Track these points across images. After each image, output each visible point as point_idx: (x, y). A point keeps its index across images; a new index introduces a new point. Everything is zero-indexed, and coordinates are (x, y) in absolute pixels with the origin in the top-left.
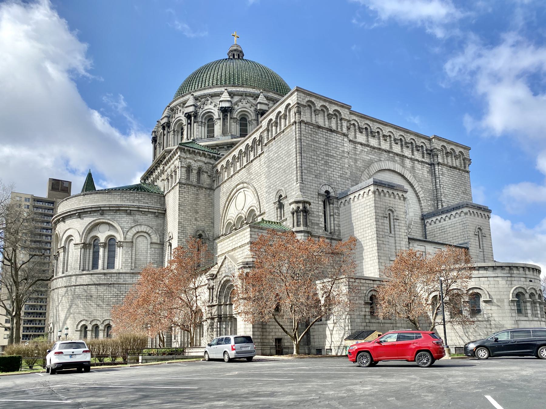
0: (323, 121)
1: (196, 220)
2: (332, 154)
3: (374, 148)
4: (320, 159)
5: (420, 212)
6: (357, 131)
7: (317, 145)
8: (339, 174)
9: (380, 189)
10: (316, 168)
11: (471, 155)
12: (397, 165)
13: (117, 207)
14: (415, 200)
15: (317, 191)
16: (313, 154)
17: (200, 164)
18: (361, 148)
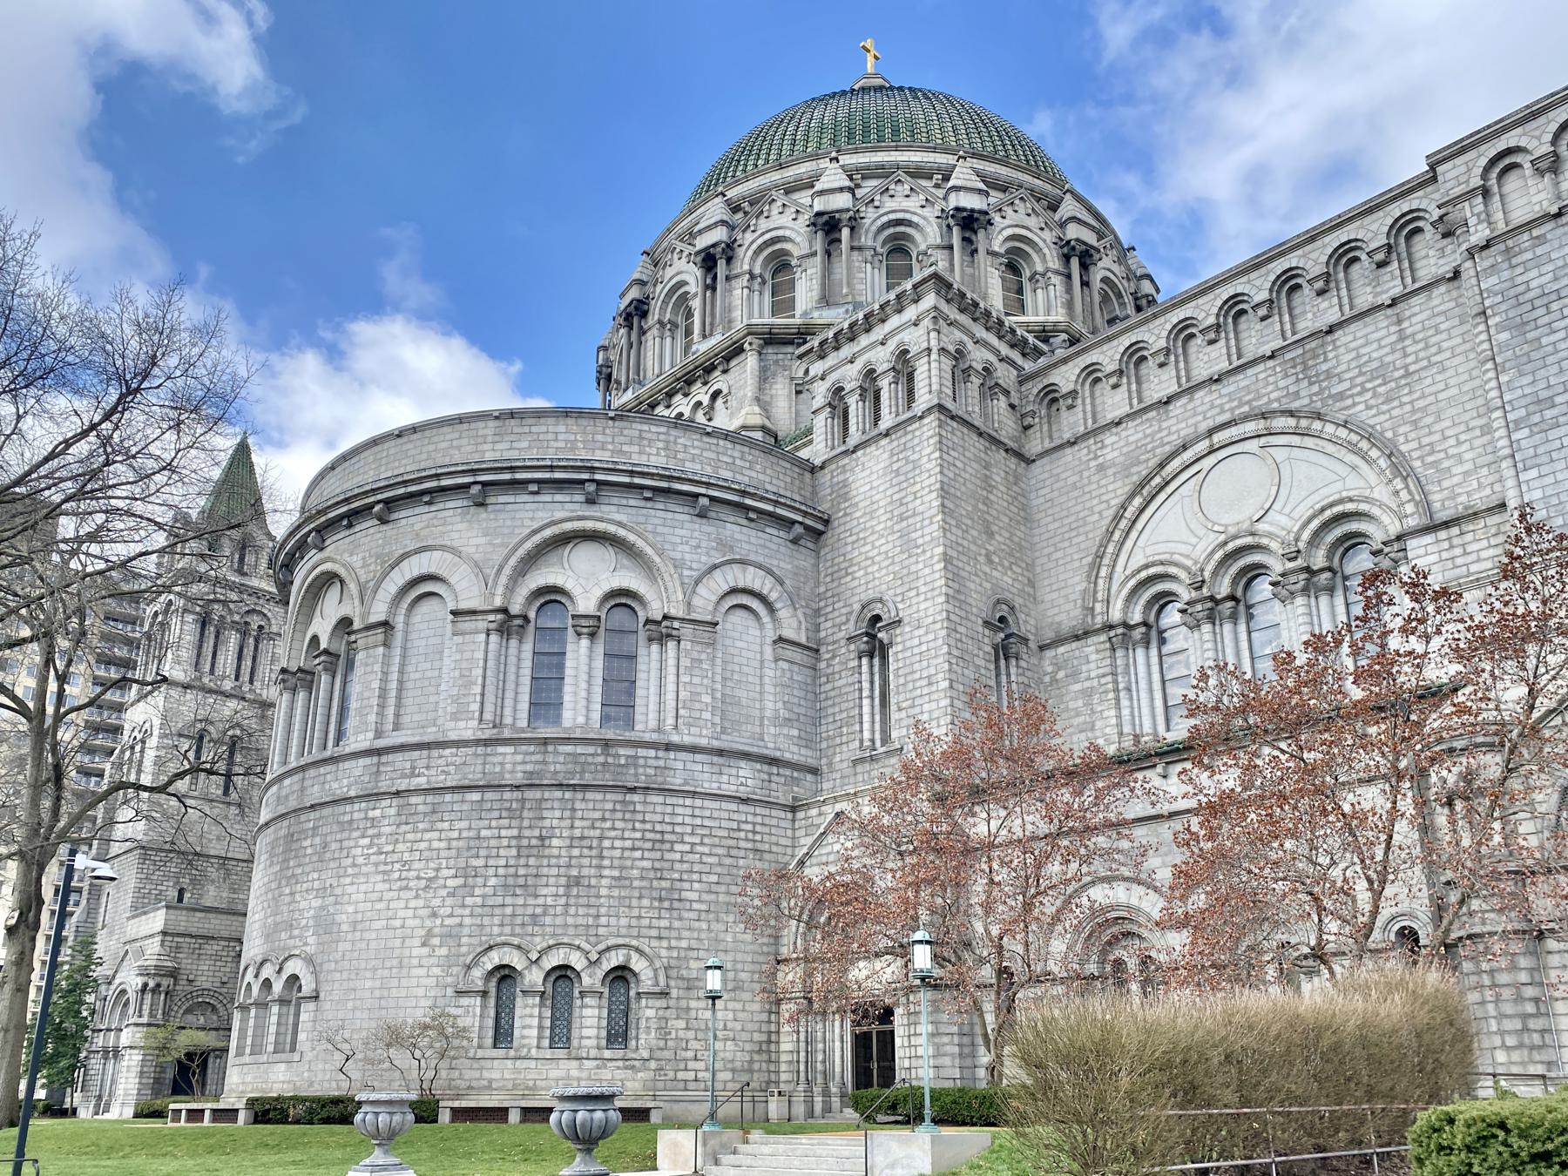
1: (990, 561)
13: (662, 477)
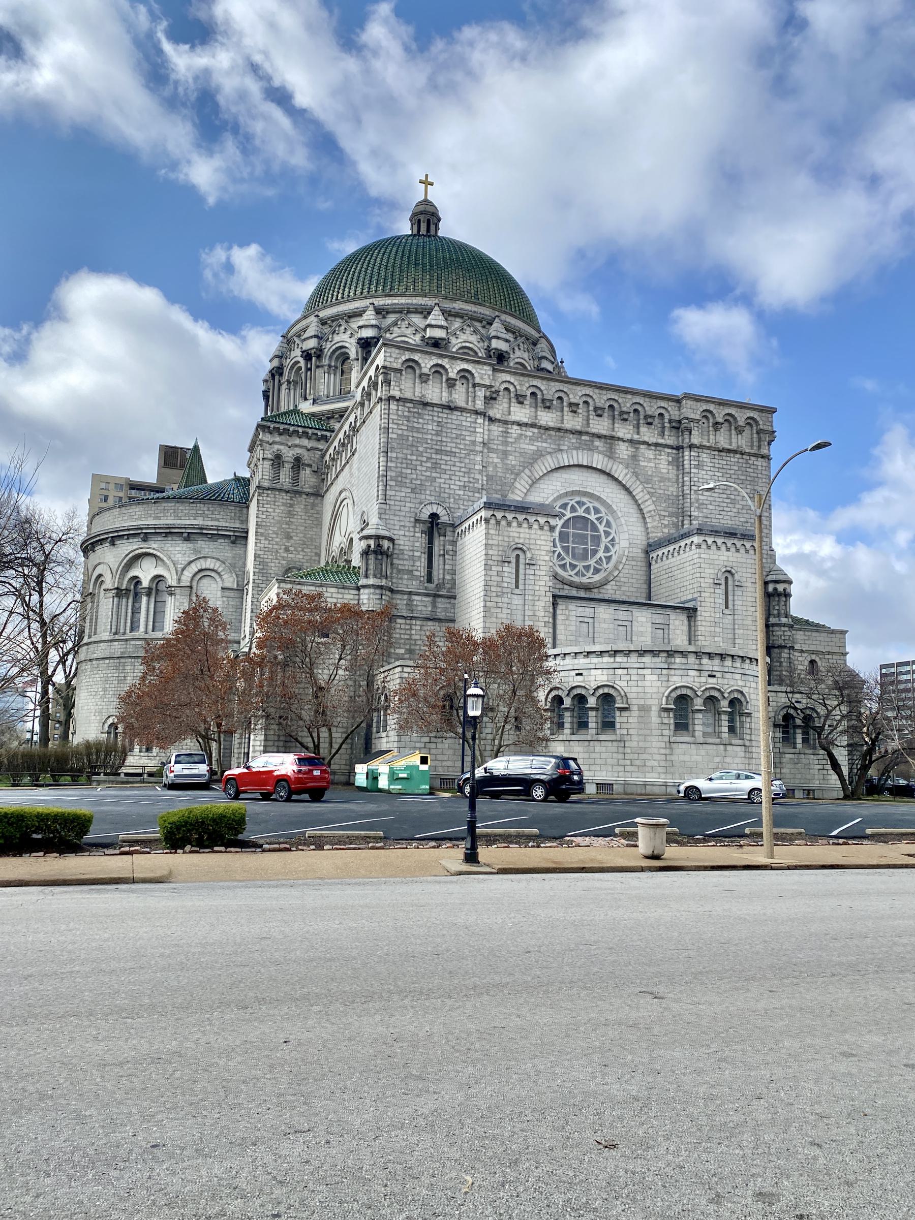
0: (438, 390)
1: (287, 550)
2: (449, 449)
3: (547, 429)
4: (425, 459)
5: (644, 538)
6: (513, 400)
8: (462, 484)
9: (499, 515)
10: (414, 476)
11: (778, 422)
12: (596, 455)
14: (634, 517)
15: (413, 515)
16: (409, 452)
17: (298, 451)
18: (519, 432)
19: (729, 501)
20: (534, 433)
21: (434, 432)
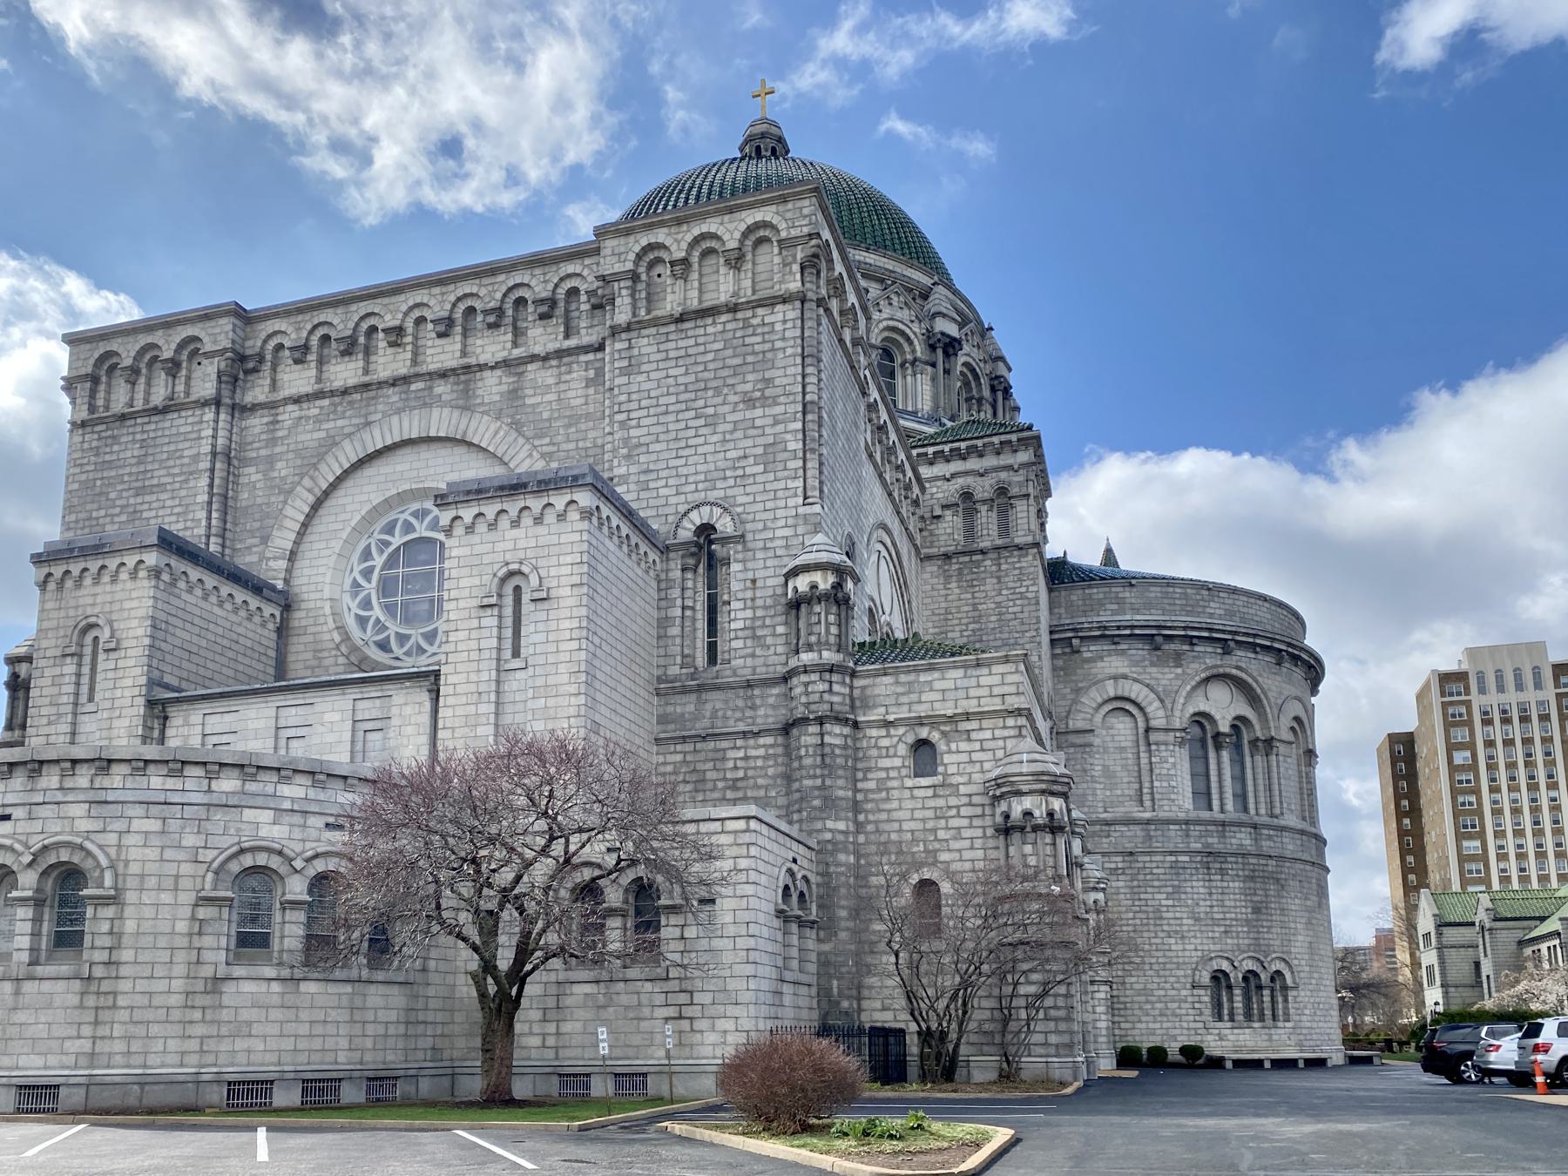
2: (155, 481)
3: (345, 392)
7: (113, 473)
18: (297, 414)
19: (702, 422)
20: (321, 408)
21: (134, 461)
